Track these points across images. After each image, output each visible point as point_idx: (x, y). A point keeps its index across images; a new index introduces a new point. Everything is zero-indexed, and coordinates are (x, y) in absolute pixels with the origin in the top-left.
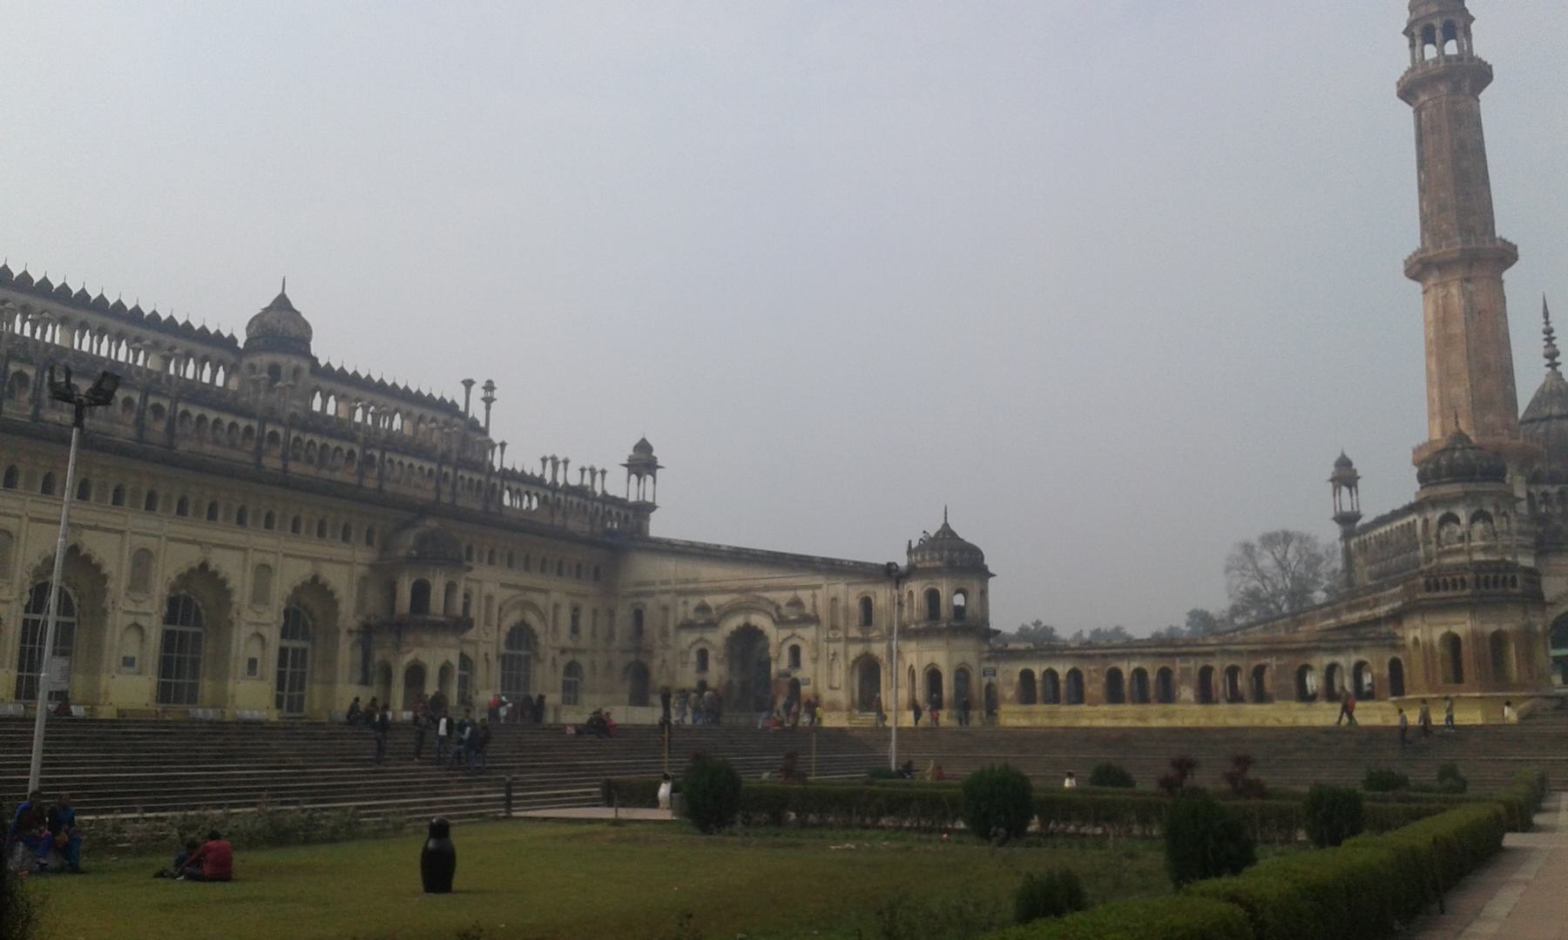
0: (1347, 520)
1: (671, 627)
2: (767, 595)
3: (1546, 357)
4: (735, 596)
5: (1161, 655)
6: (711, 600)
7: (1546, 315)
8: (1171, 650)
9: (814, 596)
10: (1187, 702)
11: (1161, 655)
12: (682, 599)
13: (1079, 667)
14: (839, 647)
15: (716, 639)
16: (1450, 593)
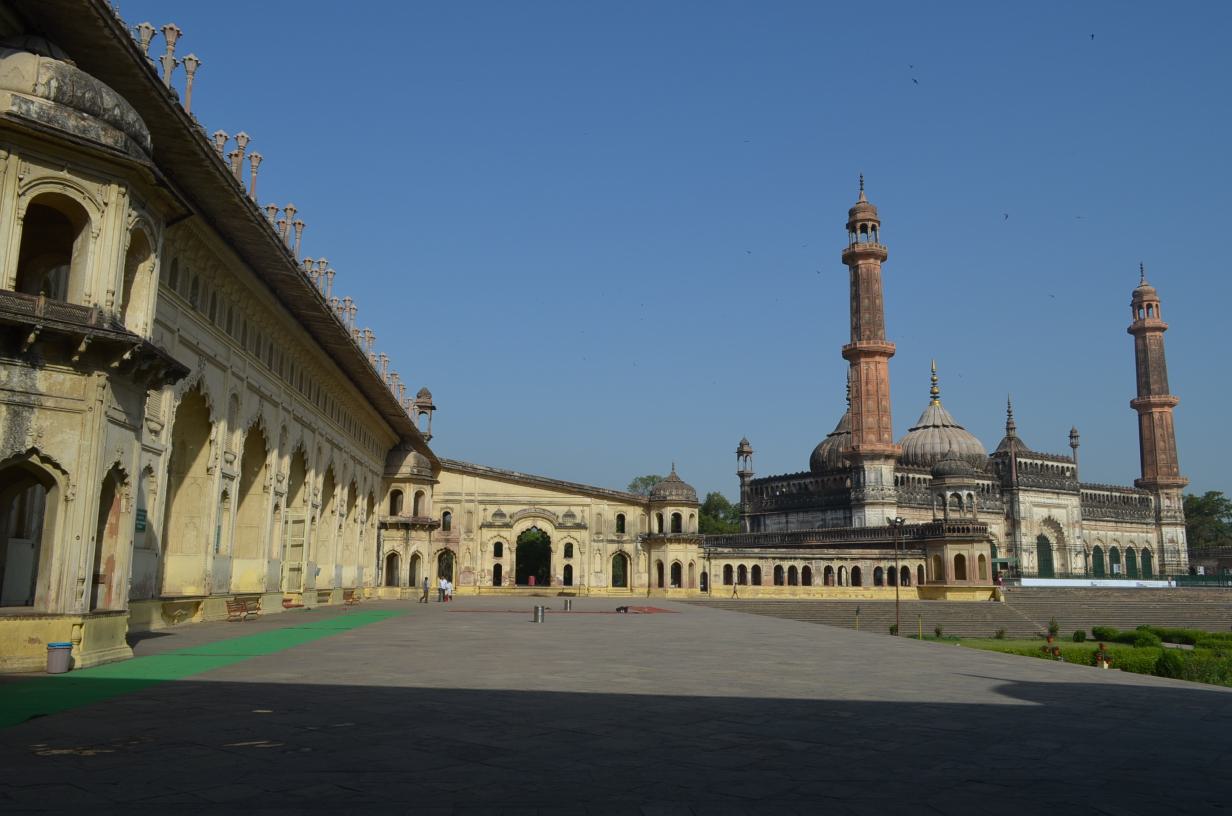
1: (475, 527)
2: (548, 508)
4: (525, 507)
6: (505, 509)
9: (582, 511)
10: (818, 585)
12: (482, 507)
13: (758, 564)
15: (510, 537)
16: (961, 534)
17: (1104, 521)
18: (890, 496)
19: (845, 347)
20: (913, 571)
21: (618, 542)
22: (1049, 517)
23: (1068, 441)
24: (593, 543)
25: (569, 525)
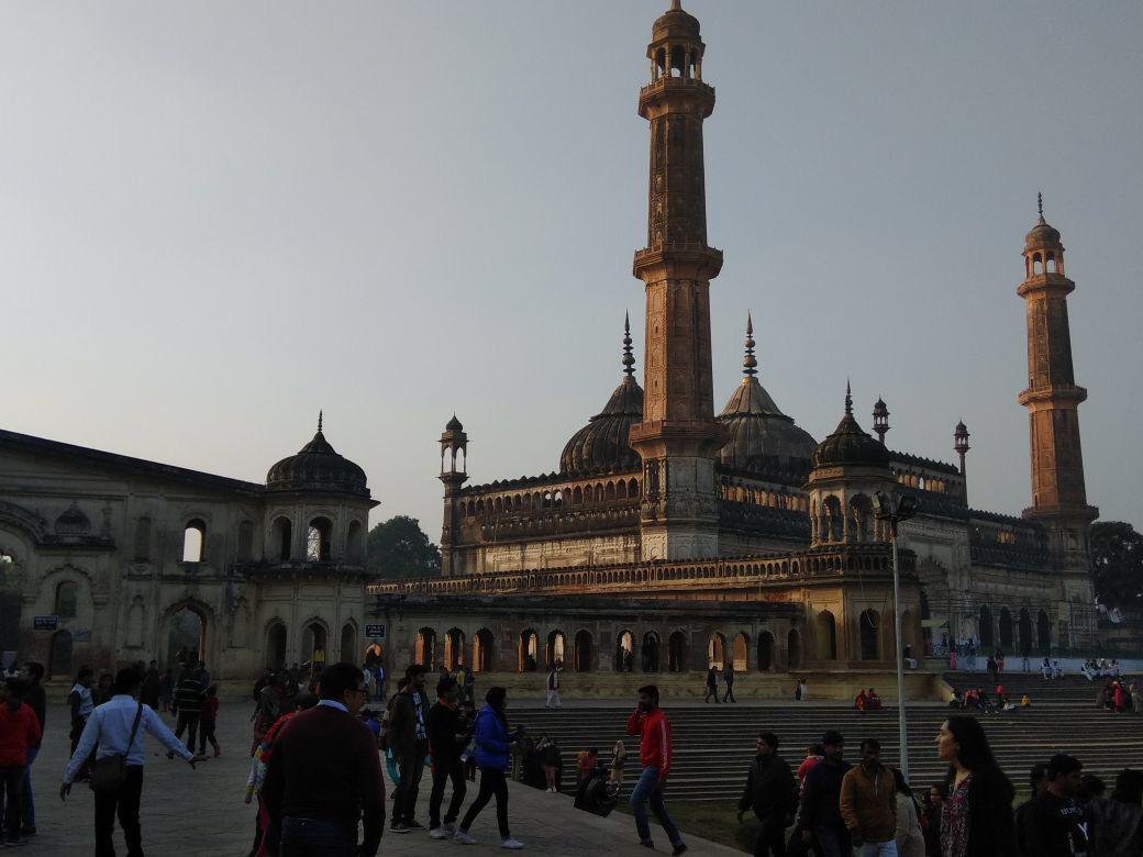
0: (453, 480)
2: (24, 502)
5: (583, 617)
7: (627, 328)
8: (592, 612)
9: (106, 511)
11: (583, 617)
14: (144, 586)
16: (872, 572)
17: (994, 567)
18: (709, 511)
19: (637, 254)
20: (780, 642)
21: (186, 580)
22: (931, 557)
23: (952, 442)
24: (125, 583)
25: (71, 540)
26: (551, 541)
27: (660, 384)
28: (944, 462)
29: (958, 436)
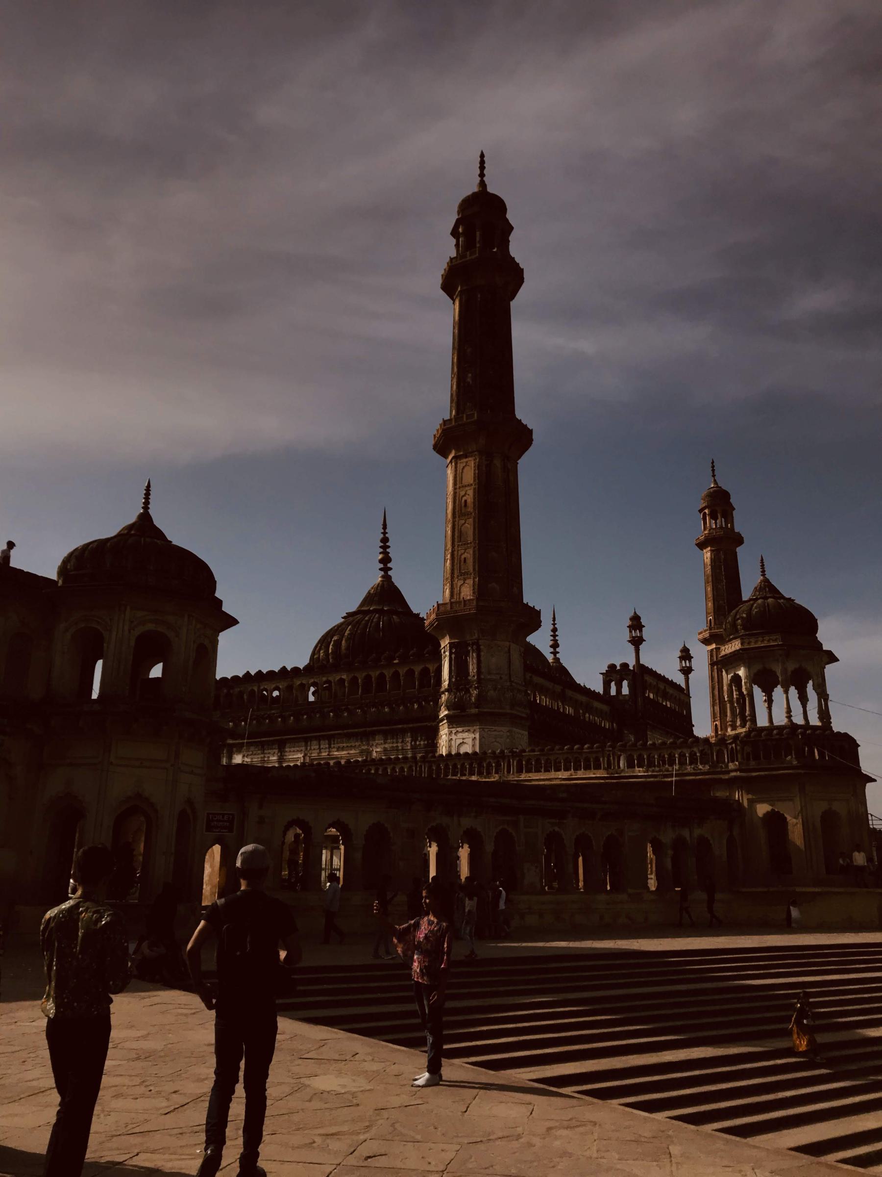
3: (381, 561)
7: (385, 526)
26: (319, 739)
27: (470, 562)
28: (674, 681)
29: (682, 658)
